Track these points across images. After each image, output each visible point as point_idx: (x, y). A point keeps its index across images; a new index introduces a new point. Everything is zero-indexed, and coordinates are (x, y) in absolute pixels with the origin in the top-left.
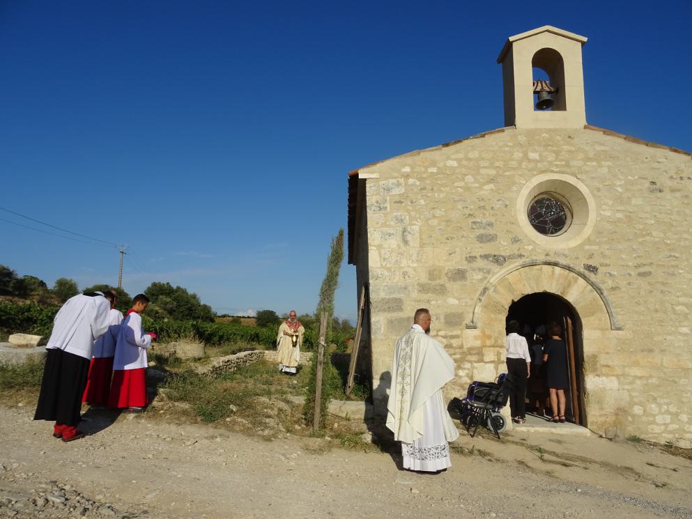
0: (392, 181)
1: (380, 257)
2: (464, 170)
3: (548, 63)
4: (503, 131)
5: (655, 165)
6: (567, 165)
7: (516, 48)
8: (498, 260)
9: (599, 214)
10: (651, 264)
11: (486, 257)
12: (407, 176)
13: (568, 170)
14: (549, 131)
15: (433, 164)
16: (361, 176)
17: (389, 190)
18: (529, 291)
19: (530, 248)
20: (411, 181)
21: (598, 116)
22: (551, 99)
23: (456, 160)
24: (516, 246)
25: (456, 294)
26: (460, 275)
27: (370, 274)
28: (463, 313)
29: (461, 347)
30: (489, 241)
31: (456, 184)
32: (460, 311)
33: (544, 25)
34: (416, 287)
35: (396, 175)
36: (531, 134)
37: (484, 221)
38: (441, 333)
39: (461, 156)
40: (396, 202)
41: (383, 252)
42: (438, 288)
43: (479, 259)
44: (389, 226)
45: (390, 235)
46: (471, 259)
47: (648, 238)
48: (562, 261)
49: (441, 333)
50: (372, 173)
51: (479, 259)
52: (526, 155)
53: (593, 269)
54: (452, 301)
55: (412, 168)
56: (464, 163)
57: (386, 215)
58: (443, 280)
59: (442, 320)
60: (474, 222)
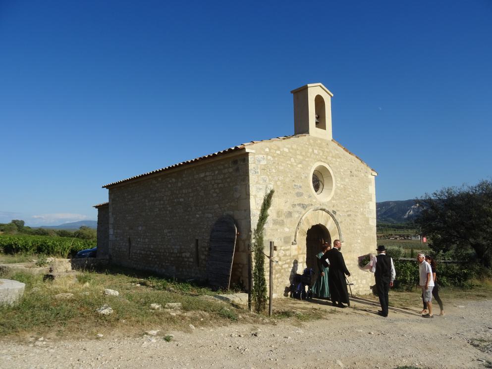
0: (261, 156)
1: (256, 202)
2: (291, 155)
3: (319, 101)
4: (305, 136)
5: (352, 163)
6: (326, 159)
7: (309, 90)
8: (304, 207)
9: (336, 185)
10: (351, 211)
11: (299, 205)
12: (267, 154)
13: (326, 161)
14: (321, 139)
15: (279, 149)
16: (247, 150)
17: (259, 161)
18: (315, 224)
19: (314, 200)
20: (269, 157)
21: (337, 137)
22: (320, 123)
23: (287, 148)
24: (310, 199)
25: (288, 226)
26: (290, 214)
27: (251, 213)
28: (290, 236)
29: (290, 255)
30: (300, 196)
31: (287, 162)
32: (289, 235)
33: (319, 82)
34: (272, 221)
35: (263, 152)
36: (315, 139)
37: (298, 185)
38: (283, 248)
39: (289, 146)
40: (262, 169)
41: (257, 200)
42: (281, 222)
43: (297, 206)
44: (259, 184)
45: (260, 189)
46: (294, 206)
47: (350, 198)
48: (327, 209)
49: (283, 248)
50: (252, 149)
51: (297, 206)
52: (313, 151)
53: (335, 212)
54: (287, 230)
55: (270, 149)
56: (291, 150)
57: (258, 176)
58: (283, 217)
59: (283, 240)
60: (295, 185)
